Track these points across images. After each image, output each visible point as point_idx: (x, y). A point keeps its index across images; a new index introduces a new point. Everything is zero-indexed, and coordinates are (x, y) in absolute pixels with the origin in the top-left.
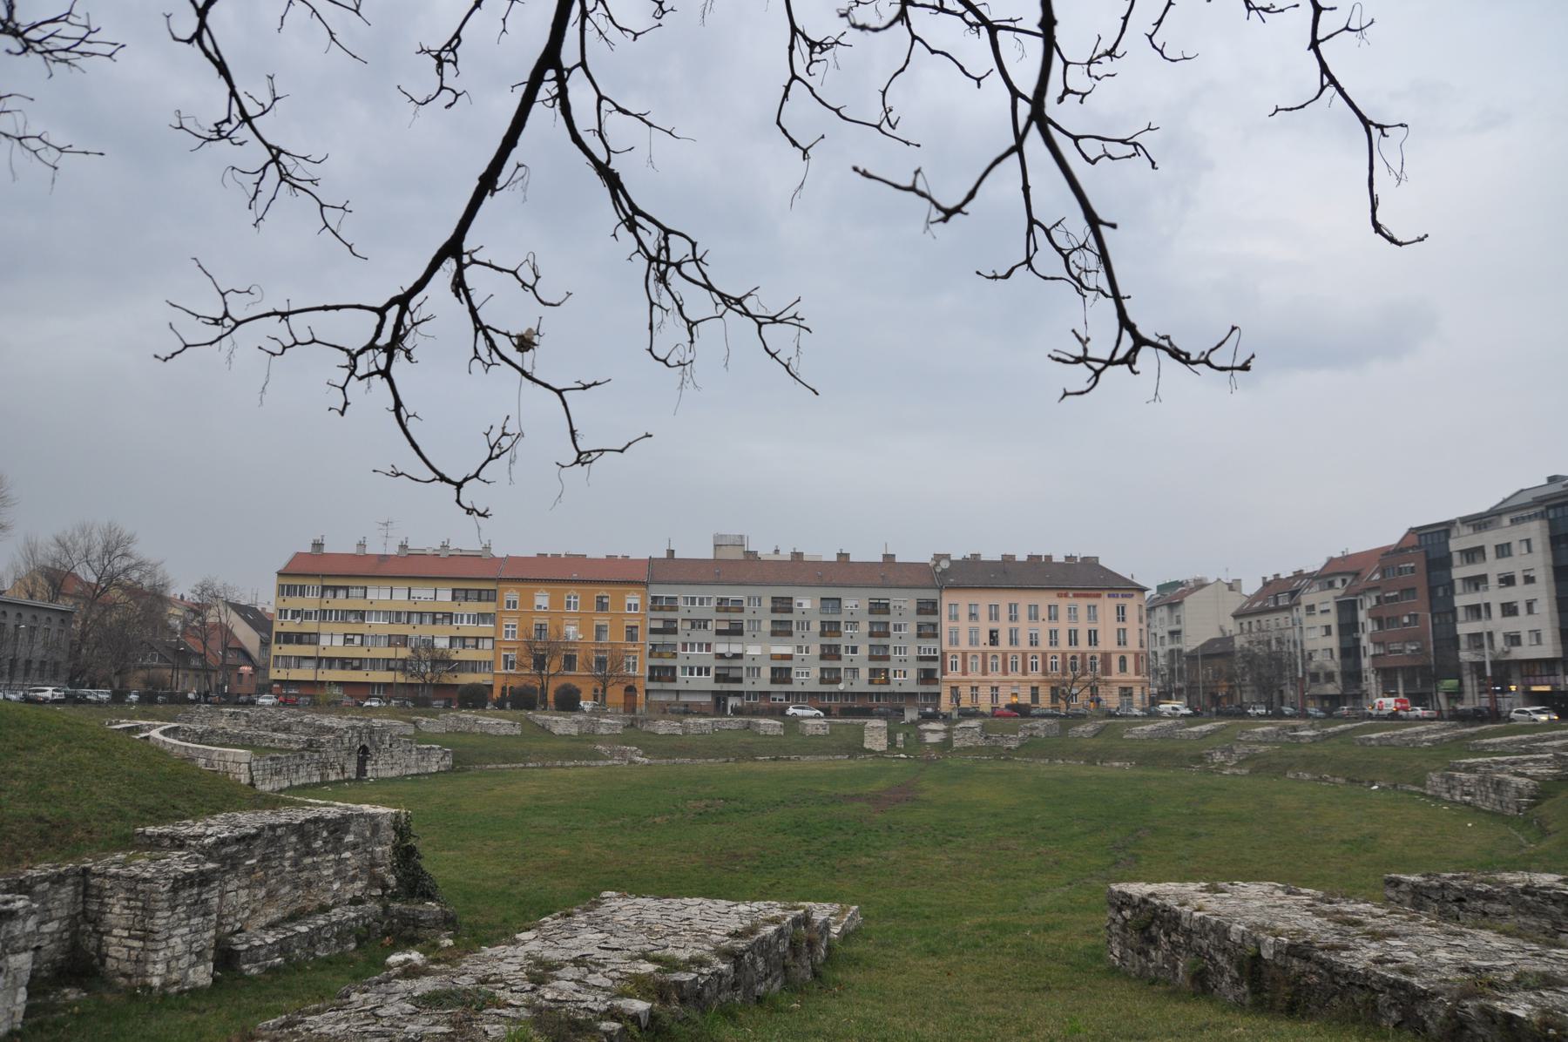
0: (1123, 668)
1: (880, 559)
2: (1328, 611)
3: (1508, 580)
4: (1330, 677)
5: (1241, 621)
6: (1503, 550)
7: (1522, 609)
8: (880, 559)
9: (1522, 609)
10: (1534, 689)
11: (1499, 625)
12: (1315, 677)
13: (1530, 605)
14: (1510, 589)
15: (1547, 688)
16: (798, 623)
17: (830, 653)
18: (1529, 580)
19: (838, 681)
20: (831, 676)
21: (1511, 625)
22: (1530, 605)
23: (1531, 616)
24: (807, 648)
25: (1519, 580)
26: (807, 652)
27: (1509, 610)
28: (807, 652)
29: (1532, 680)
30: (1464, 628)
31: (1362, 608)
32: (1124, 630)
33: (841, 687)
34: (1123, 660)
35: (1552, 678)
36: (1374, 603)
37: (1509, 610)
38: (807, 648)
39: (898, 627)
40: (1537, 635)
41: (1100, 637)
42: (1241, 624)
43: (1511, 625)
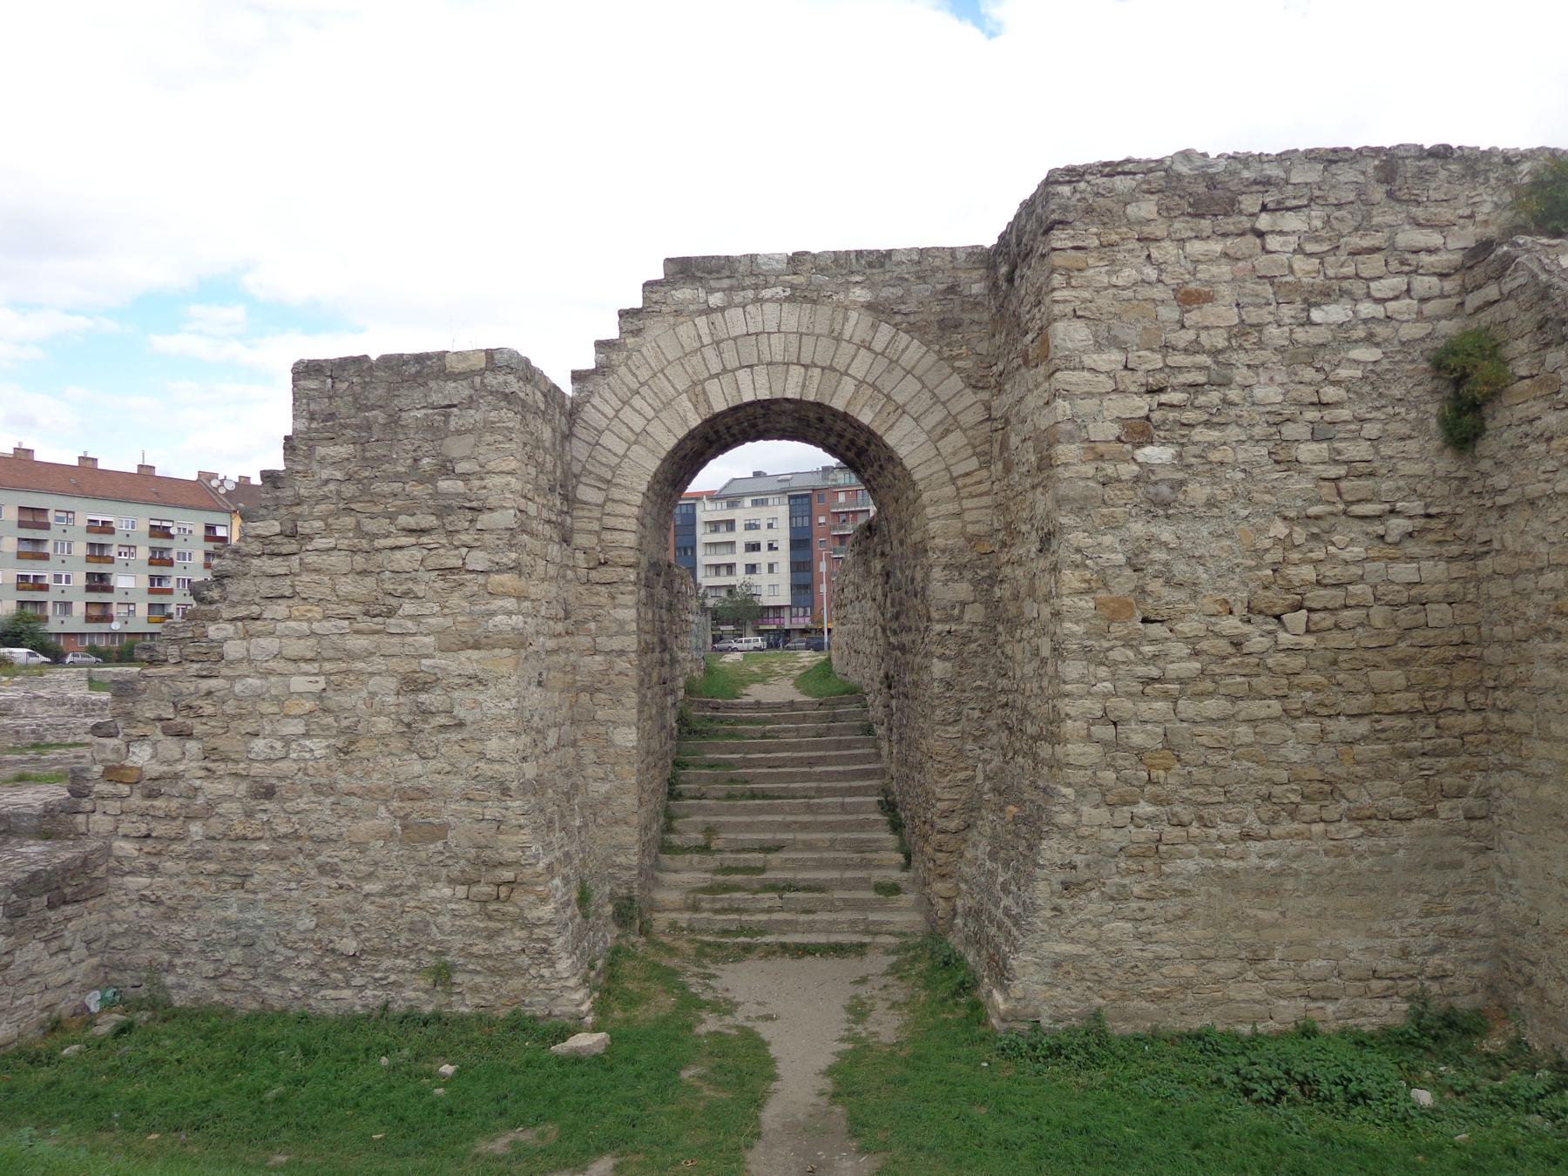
1: (135, 471)
3: (754, 547)
6: (751, 526)
7: (765, 569)
8: (135, 471)
11: (740, 576)
13: (771, 567)
14: (755, 554)
16: (56, 544)
17: (98, 583)
18: (771, 547)
19: (109, 619)
20: (100, 613)
22: (771, 567)
24: (68, 578)
25: (764, 547)
26: (68, 581)
28: (68, 581)
33: (116, 626)
38: (68, 578)
39: (182, 556)
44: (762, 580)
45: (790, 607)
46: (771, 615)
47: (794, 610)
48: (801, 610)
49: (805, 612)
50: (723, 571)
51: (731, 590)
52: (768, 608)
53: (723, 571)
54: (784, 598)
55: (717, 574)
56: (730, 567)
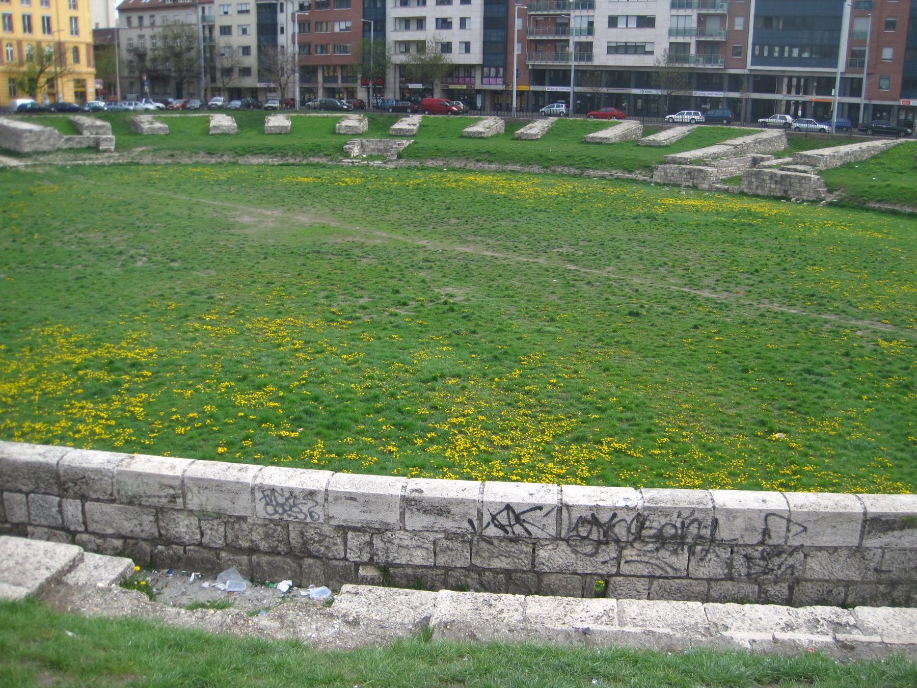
0: (77, 59)
2: (247, 11)
4: (246, 72)
5: (129, 14)
7: (456, 24)
9: (456, 24)
10: (451, 87)
11: (430, 34)
12: (228, 72)
13: (463, 21)
15: (464, 87)
21: (445, 35)
22: (463, 21)
23: (463, 31)
27: (444, 23)
29: (449, 80)
30: (394, 35)
31: (282, 11)
32: (76, 19)
34: (76, 50)
35: (467, 79)
36: (297, 8)
37: (444, 23)
40: (467, 47)
41: (54, 26)
42: (129, 19)
43: (445, 35)
44: (454, 36)
45: (482, 66)
46: (462, 74)
47: (486, 70)
48: (493, 70)
49: (497, 72)
50: (413, 25)
51: (421, 45)
52: (458, 67)
53: (413, 25)
54: (475, 57)
55: (407, 27)
56: (420, 22)
